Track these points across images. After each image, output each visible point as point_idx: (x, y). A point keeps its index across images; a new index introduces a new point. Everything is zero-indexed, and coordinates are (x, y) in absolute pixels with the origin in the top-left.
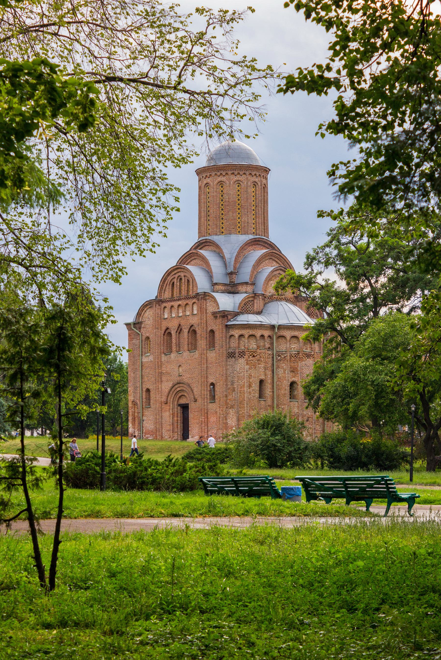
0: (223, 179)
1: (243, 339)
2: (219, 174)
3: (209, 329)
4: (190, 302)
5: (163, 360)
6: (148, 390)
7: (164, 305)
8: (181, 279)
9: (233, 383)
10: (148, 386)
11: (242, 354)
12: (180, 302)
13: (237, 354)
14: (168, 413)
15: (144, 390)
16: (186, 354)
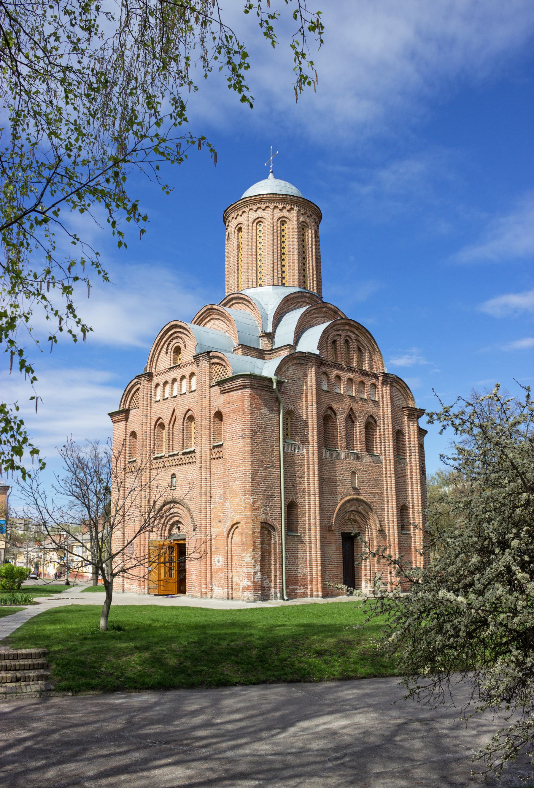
4: (368, 382)
12: (350, 375)
14: (333, 547)
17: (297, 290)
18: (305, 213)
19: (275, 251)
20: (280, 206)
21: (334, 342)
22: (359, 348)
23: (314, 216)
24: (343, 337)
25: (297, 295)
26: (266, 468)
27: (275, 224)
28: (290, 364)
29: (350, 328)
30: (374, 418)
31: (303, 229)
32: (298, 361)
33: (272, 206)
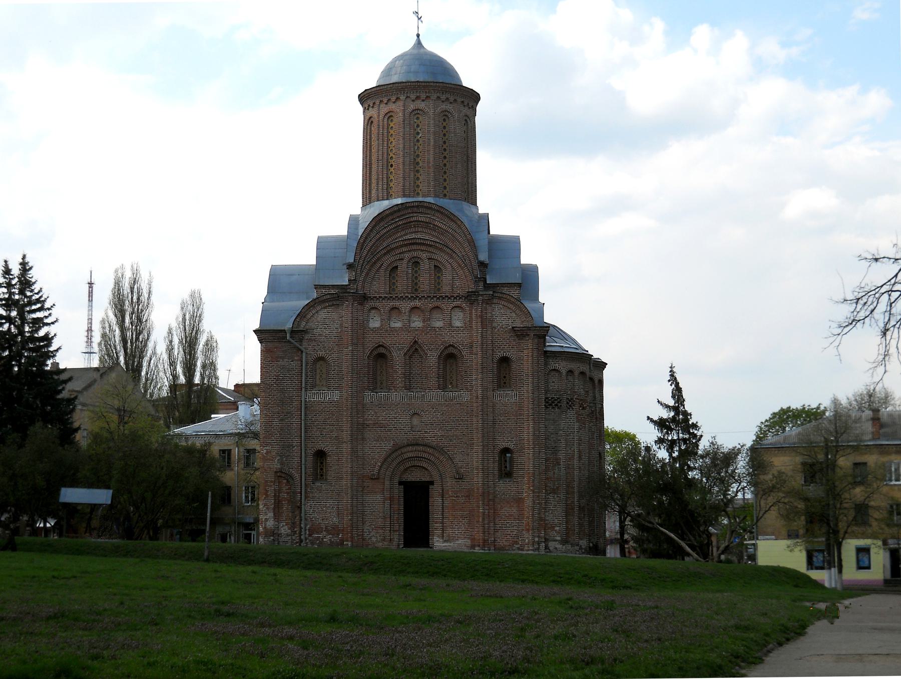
0: (449, 107)
1: (570, 378)
2: (443, 97)
3: (499, 354)
4: (447, 305)
5: (367, 400)
6: (321, 455)
7: (372, 304)
8: (416, 264)
9: (555, 451)
10: (321, 446)
11: (570, 403)
12: (417, 303)
13: (564, 404)
14: (379, 497)
15: (311, 452)
16: (434, 395)
17: (399, 201)
18: (418, 98)
19: (380, 158)
20: (385, 101)
21: (397, 267)
22: (435, 266)
23: (434, 96)
24: (405, 261)
25: (396, 208)
26: (282, 420)
27: (381, 124)
28: (319, 308)
29: (419, 247)
30: (456, 348)
31: (418, 118)
32: (331, 303)
33: (377, 102)
